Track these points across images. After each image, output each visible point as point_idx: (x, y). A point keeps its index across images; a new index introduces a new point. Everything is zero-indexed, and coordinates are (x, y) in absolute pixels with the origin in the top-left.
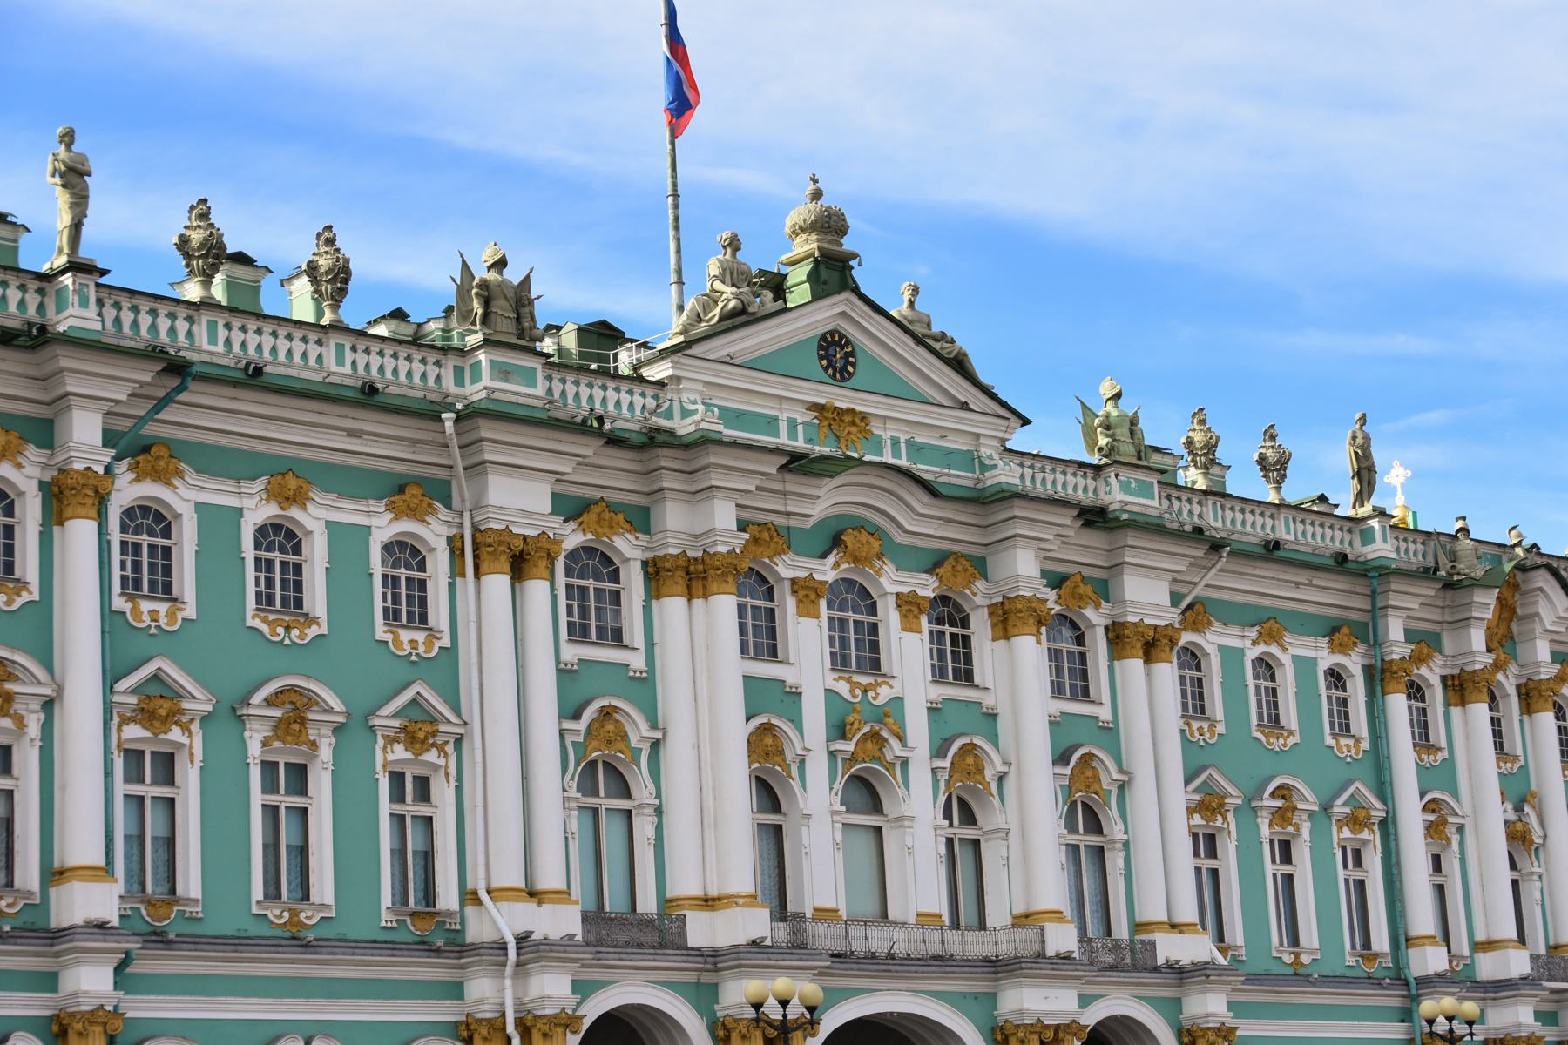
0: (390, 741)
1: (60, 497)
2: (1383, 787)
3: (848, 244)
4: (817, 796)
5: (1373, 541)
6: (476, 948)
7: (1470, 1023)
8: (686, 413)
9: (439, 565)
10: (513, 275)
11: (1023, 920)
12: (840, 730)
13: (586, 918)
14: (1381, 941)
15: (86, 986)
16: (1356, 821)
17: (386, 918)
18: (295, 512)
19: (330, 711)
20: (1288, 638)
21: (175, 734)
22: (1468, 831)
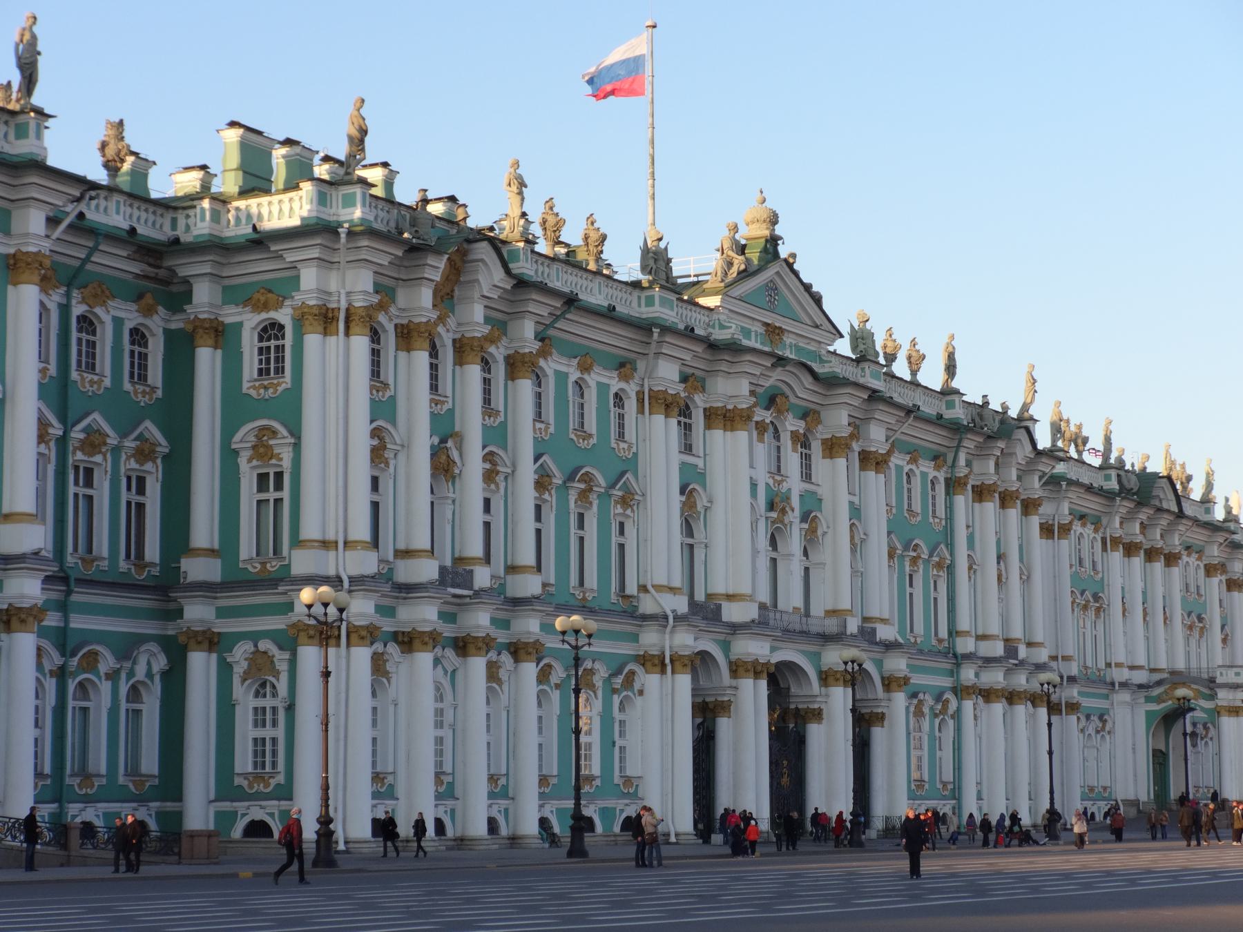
0: (616, 502)
1: (516, 365)
2: (951, 546)
3: (779, 230)
4: (763, 542)
5: (954, 407)
6: (645, 618)
7: (1055, 686)
8: (722, 327)
9: (631, 405)
10: (662, 245)
11: (831, 613)
12: (771, 506)
13: (692, 603)
14: (943, 633)
15: (532, 629)
16: (939, 566)
17: (614, 598)
18: (586, 377)
19: (599, 486)
20: (921, 461)
21: (546, 496)
22: (978, 573)
